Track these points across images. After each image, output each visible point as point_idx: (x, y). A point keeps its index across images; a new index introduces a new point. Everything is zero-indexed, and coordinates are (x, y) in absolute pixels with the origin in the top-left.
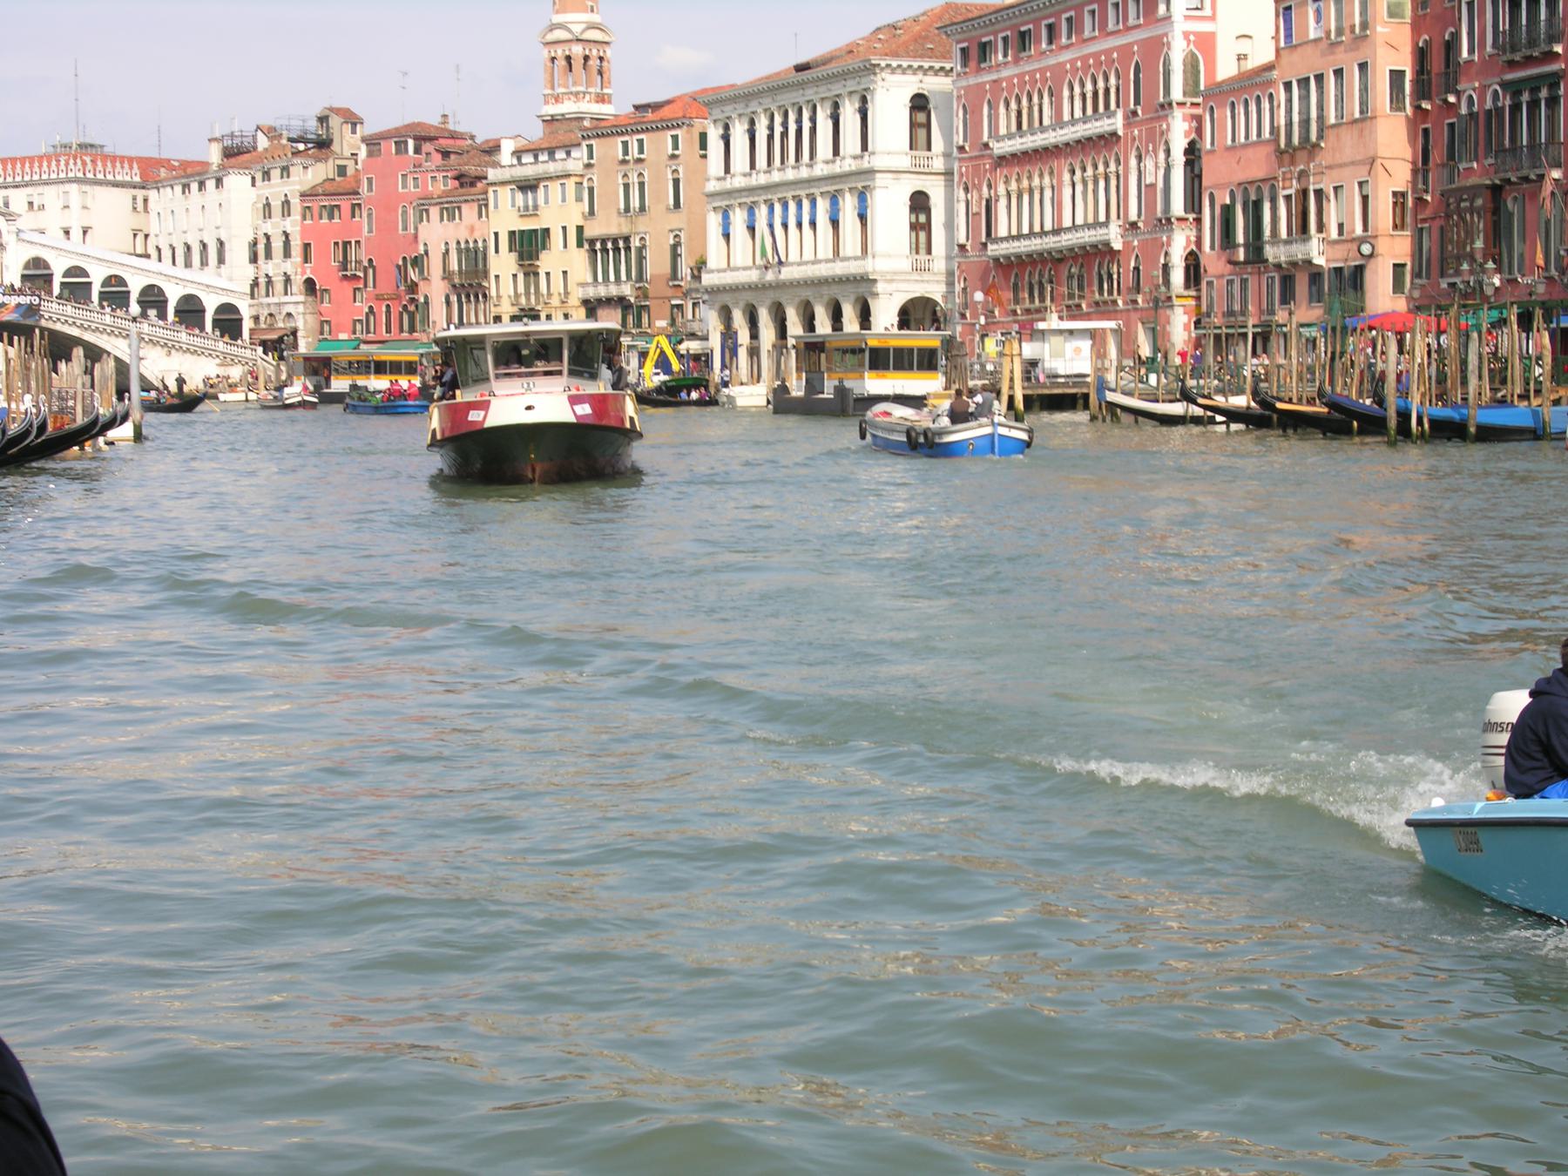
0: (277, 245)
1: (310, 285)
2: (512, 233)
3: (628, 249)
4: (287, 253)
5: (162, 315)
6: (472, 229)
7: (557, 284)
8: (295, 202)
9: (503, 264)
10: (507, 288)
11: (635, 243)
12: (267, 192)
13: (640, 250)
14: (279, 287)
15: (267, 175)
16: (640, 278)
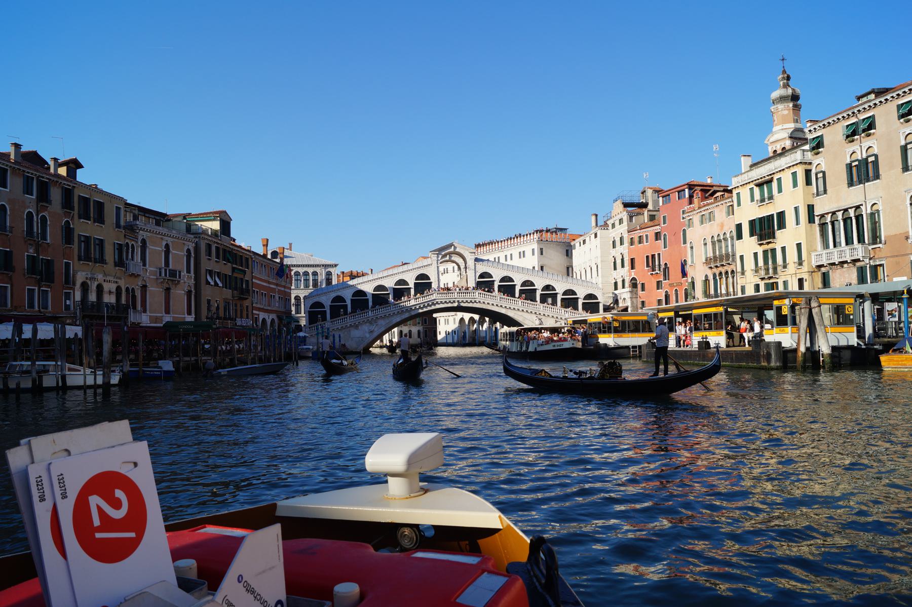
1: (634, 285)
2: (752, 223)
3: (859, 218)
4: (623, 266)
5: (554, 303)
6: (722, 226)
9: (749, 246)
10: (749, 264)
11: (865, 211)
12: (613, 235)
14: (620, 285)
16: (875, 238)
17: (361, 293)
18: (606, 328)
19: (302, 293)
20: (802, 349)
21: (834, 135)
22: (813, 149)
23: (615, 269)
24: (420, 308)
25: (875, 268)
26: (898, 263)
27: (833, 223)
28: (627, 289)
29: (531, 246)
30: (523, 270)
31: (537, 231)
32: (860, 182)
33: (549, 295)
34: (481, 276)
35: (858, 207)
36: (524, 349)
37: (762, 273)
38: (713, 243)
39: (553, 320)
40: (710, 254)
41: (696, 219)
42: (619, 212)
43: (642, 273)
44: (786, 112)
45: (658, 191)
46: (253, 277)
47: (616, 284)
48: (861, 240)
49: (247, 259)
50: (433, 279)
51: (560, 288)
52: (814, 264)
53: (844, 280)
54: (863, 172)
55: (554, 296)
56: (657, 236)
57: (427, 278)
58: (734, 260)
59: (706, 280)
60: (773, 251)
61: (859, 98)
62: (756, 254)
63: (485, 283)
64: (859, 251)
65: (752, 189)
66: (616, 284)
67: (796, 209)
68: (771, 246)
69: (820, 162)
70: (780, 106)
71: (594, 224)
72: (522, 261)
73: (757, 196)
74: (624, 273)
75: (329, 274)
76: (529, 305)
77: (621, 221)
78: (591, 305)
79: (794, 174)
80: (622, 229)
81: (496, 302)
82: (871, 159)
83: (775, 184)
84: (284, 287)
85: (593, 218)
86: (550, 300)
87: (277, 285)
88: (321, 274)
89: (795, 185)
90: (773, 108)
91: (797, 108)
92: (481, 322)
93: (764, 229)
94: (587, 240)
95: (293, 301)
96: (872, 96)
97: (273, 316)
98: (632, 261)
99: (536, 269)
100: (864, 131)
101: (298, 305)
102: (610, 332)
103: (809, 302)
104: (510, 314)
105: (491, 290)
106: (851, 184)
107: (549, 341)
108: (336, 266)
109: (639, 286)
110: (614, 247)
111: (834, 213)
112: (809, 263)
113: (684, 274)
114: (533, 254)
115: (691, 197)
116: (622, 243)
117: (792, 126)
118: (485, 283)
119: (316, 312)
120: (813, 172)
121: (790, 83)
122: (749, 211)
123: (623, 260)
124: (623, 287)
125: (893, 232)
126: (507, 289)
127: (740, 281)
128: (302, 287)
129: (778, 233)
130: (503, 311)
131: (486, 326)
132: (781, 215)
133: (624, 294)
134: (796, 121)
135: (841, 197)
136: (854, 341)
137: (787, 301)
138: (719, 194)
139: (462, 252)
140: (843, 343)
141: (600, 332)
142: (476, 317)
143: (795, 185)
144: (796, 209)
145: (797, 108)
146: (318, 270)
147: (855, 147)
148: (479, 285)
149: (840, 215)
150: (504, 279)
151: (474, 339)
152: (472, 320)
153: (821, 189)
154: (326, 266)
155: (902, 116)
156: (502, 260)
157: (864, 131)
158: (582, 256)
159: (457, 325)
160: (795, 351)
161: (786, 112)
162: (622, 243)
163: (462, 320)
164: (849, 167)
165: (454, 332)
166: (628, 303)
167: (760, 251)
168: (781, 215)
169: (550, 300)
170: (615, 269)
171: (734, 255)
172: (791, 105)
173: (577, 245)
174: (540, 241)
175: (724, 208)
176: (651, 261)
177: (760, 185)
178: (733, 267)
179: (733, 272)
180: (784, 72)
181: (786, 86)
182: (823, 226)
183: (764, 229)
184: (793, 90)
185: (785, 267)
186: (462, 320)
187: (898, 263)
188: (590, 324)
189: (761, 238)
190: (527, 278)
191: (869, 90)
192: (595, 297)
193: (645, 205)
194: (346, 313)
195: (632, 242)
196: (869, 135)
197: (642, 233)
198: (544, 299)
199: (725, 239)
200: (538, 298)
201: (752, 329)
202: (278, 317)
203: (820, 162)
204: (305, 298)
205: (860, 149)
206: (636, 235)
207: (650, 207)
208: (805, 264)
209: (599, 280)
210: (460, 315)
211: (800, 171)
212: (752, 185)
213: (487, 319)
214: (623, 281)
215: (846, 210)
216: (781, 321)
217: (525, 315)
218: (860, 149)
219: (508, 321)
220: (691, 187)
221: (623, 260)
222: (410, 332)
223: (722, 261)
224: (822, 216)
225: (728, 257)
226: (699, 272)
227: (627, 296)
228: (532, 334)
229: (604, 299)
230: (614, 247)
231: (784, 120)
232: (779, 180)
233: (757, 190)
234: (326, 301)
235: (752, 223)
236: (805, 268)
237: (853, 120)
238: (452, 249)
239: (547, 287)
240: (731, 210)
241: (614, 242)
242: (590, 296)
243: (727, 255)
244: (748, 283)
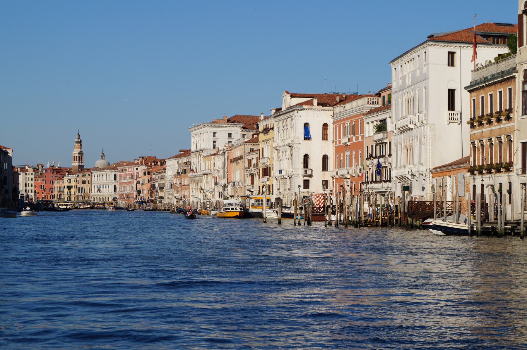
1: (35, 192)
8: (33, 178)
9: (66, 190)
10: (66, 194)
14: (30, 191)
28: (33, 193)
42: (30, 170)
45: (43, 166)
56: (43, 180)
80: (33, 176)
122: (67, 184)
176: (41, 187)
183: (69, 188)
193: (38, 169)
195: (35, 180)
197: (39, 179)
207: (40, 170)
223: (61, 192)
240: (63, 183)
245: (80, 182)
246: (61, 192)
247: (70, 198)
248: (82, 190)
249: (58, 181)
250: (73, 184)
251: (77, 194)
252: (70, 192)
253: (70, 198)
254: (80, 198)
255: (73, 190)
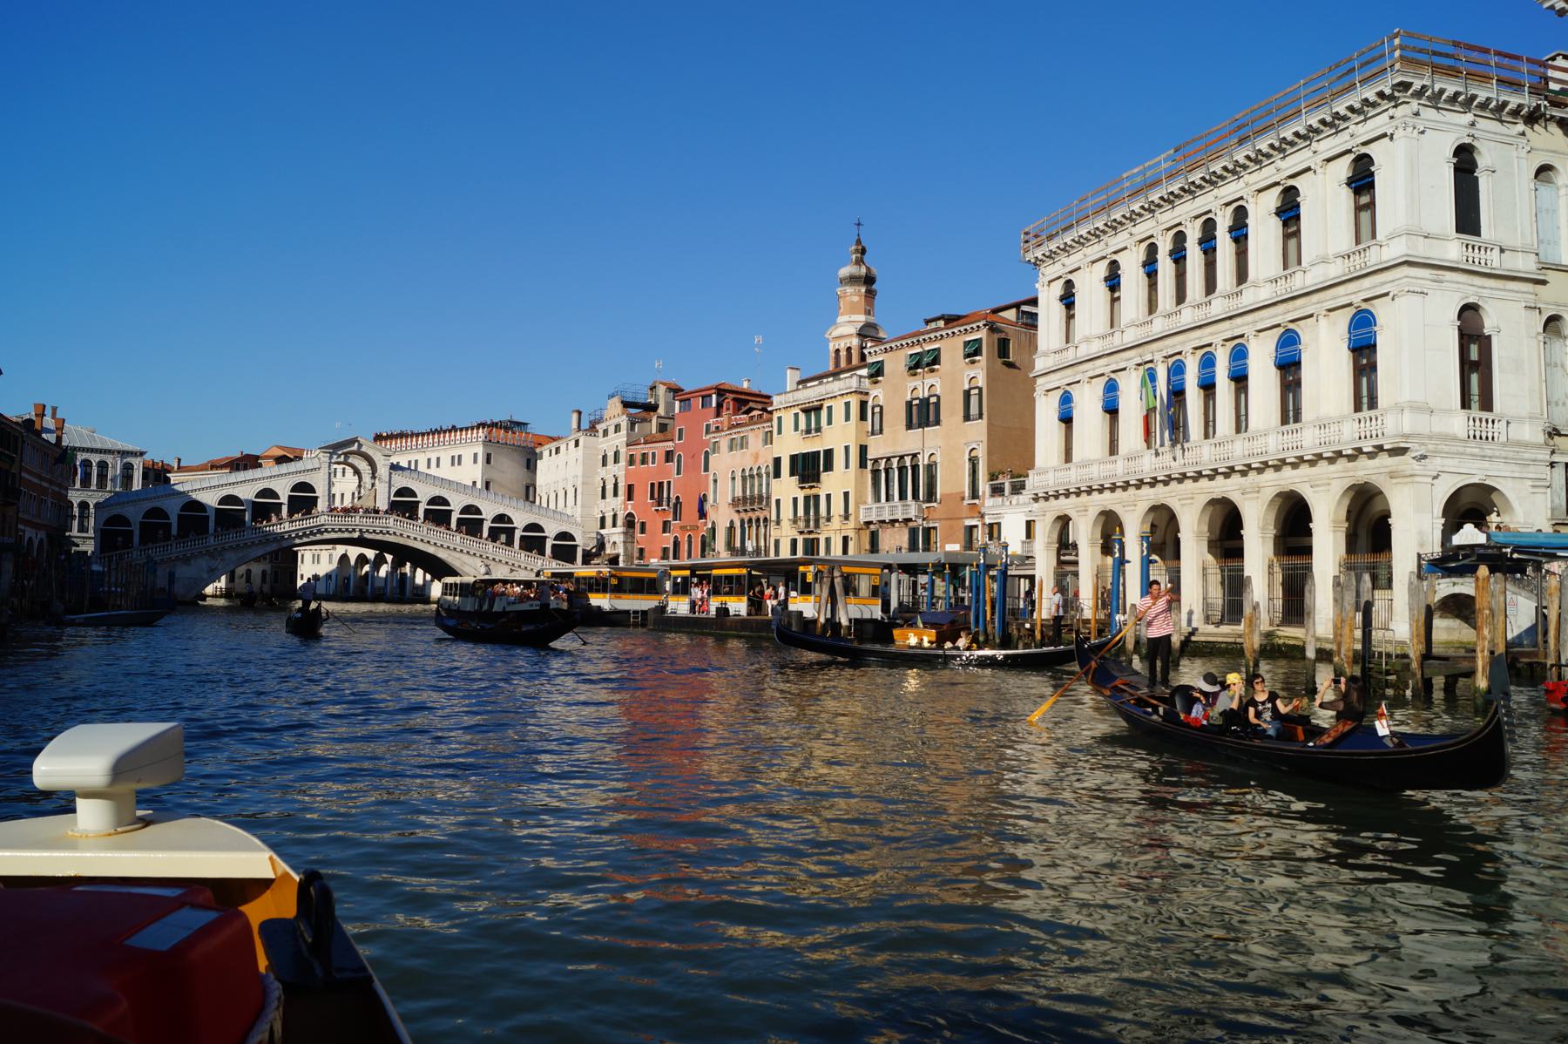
0: (610, 488)
1: (630, 522)
2: (793, 458)
3: (915, 468)
4: (616, 494)
5: (510, 543)
6: (757, 457)
7: (838, 507)
8: (623, 450)
9: (787, 489)
10: (787, 512)
11: (923, 461)
12: (604, 446)
13: (931, 468)
14: (609, 521)
15: (606, 433)
16: (931, 495)
17: (198, 506)
18: (599, 585)
19: (94, 497)
20: (822, 620)
21: (896, 363)
22: (871, 376)
23: (604, 497)
24: (297, 536)
25: (927, 531)
26: (951, 527)
27: (887, 471)
28: (620, 529)
29: (472, 448)
30: (458, 487)
31: (483, 425)
32: (920, 426)
33: (502, 530)
34: (400, 493)
35: (915, 456)
36: (485, 607)
37: (802, 524)
38: (744, 479)
39: (507, 569)
40: (739, 493)
41: (724, 444)
42: (614, 413)
43: (642, 506)
44: (856, 299)
45: (675, 391)
46: (21, 469)
47: (603, 519)
48: (915, 496)
49: (16, 438)
50: (321, 491)
51: (520, 519)
52: (862, 519)
53: (894, 543)
54: (923, 414)
55: (510, 532)
56: (669, 456)
57: (311, 489)
58: (768, 504)
59: (731, 528)
60: (817, 497)
61: (928, 322)
62: (795, 500)
63: (404, 505)
64: (912, 509)
65: (796, 415)
66: (603, 519)
67: (847, 448)
68: (814, 491)
69: (878, 394)
70: (849, 290)
71: (575, 425)
72: (456, 469)
73: (802, 425)
74: (616, 505)
75: (128, 468)
76: (471, 543)
77: (617, 428)
78: (565, 550)
79: (847, 405)
80: (619, 440)
81: (418, 535)
82: (933, 400)
83: (824, 413)
84: (60, 486)
85: (575, 416)
86: (503, 538)
87: (51, 482)
88: (114, 467)
89: (847, 418)
90: (839, 290)
91: (871, 294)
92: (379, 561)
93: (809, 468)
94: (563, 448)
95: (76, 511)
96: (941, 323)
97: (42, 535)
98: (630, 488)
99: (479, 485)
100: (928, 365)
101: (83, 516)
102: (605, 591)
103: (831, 571)
104: (442, 554)
105: (413, 516)
106: (909, 426)
107: (522, 598)
108: (142, 454)
109: (638, 526)
110: (604, 464)
111: (888, 459)
112: (857, 517)
113: (702, 514)
114: (475, 461)
115: (719, 406)
116: (616, 460)
117: (862, 318)
118: (404, 505)
119: (113, 532)
120: (870, 404)
121: (866, 258)
122: (790, 443)
123: (616, 485)
124: (614, 525)
125: (949, 490)
126: (438, 515)
127: (774, 533)
128: (93, 487)
129: (824, 476)
130: (431, 550)
131: (384, 571)
132: (829, 453)
133: (615, 537)
134: (868, 313)
135: (896, 441)
136: (878, 614)
137: (811, 568)
138: (755, 413)
139: (370, 452)
140: (867, 616)
141: (591, 590)
142: (371, 554)
143: (847, 418)
144: (847, 448)
145: (871, 294)
146: (109, 459)
147: (916, 382)
148: (395, 507)
149: (895, 462)
150: (435, 500)
151: (363, 591)
152: (362, 559)
153: (877, 427)
154: (124, 453)
155: (967, 356)
156: (422, 468)
157: (928, 365)
158: (553, 471)
159: (334, 565)
160: (814, 621)
161: (856, 299)
162: (616, 460)
163: (344, 558)
164: (909, 405)
165: (328, 576)
166: (620, 550)
167: (801, 495)
168: (829, 453)
169: (503, 538)
170: (604, 497)
171: (768, 498)
172: (863, 290)
173: (546, 453)
174: (488, 442)
175: (761, 436)
176: (657, 492)
177: (806, 411)
178: (766, 513)
179: (765, 520)
180: (859, 242)
181: (859, 262)
182: (875, 472)
183: (809, 468)
184: (868, 269)
185: (829, 520)
186: (344, 558)
187: (951, 527)
188: (578, 579)
189: (803, 480)
190: (470, 501)
191: (938, 314)
192: (572, 538)
193: (654, 408)
194: (168, 536)
195: (631, 461)
196: (932, 371)
197: (648, 449)
198: (494, 535)
199: (759, 475)
200: (485, 534)
201: (776, 596)
202: (48, 536)
203: (878, 394)
204: (97, 505)
205: (923, 386)
206: (638, 451)
207: (661, 411)
208: (852, 518)
209: (578, 511)
210: (341, 549)
211: (854, 402)
212: (797, 410)
213: (389, 558)
214: (615, 516)
215: (902, 457)
216: (806, 590)
217: (465, 558)
218: (923, 386)
219: (439, 568)
220: (721, 392)
221: (616, 485)
222: (249, 572)
223: (752, 503)
224: (876, 461)
225: (761, 500)
226: (722, 515)
227: (619, 539)
228: (499, 588)
229: (583, 541)
230: (604, 464)
231: (853, 311)
232: (830, 408)
233: (802, 417)
234: (135, 515)
235: (793, 458)
236: (851, 524)
237: (918, 350)
238: (355, 447)
239: (501, 518)
240: (768, 439)
241: (605, 457)
242: (564, 536)
243: (761, 497)
244: (783, 539)
245: (895, 416)
246: (752, 503)
247: (811, 546)
248: (913, 478)
249: (736, 434)
250: (839, 435)
251: (869, 510)
252: (812, 502)
253: (811, 546)
254: (894, 543)
255: (834, 483)
